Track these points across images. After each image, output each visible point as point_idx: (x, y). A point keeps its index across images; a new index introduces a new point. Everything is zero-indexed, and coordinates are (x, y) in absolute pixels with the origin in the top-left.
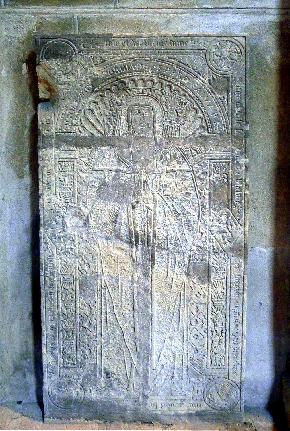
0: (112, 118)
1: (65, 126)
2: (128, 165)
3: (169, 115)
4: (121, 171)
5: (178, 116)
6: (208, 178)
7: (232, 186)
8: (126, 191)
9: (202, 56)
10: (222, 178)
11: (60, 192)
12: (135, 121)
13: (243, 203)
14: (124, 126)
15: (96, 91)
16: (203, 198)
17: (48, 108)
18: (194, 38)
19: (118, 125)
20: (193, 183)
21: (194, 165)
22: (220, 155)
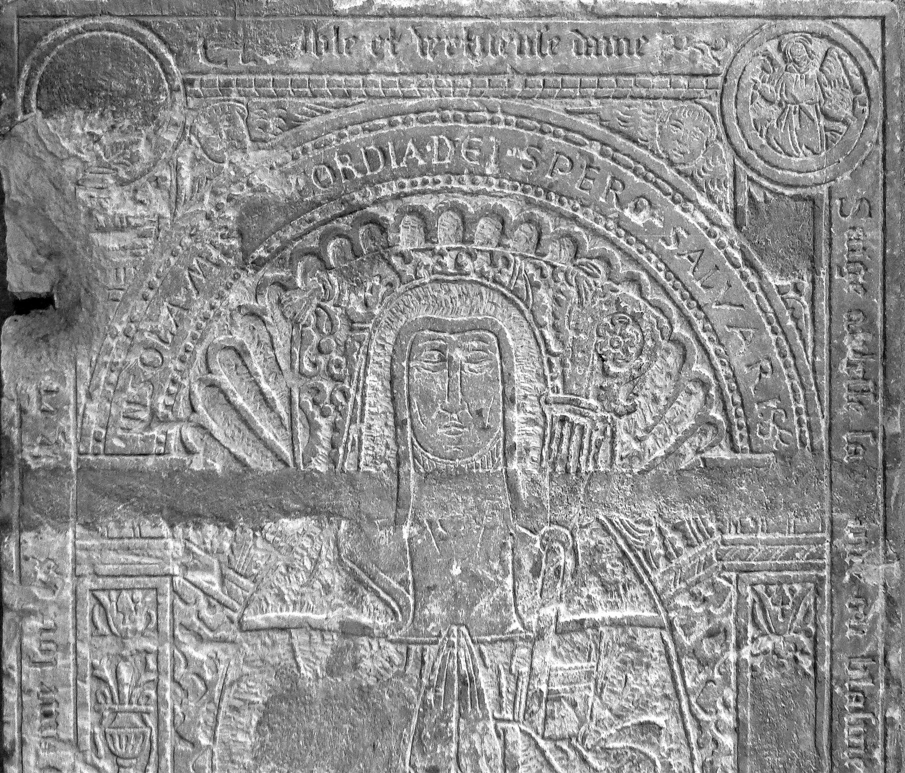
0: (328, 387)
1: (124, 422)
2: (393, 604)
3: (569, 370)
4: (365, 630)
5: (605, 373)
6: (732, 656)
7: (832, 689)
8: (382, 724)
9: (705, 101)
10: (790, 654)
11: (97, 730)
12: (426, 399)
13: (880, 762)
14: (377, 424)
15: (258, 264)
16: (711, 746)
17: (45, 338)
18: (674, 23)
19: (353, 421)
20: (669, 679)
21: (672, 598)
22: (780, 551)
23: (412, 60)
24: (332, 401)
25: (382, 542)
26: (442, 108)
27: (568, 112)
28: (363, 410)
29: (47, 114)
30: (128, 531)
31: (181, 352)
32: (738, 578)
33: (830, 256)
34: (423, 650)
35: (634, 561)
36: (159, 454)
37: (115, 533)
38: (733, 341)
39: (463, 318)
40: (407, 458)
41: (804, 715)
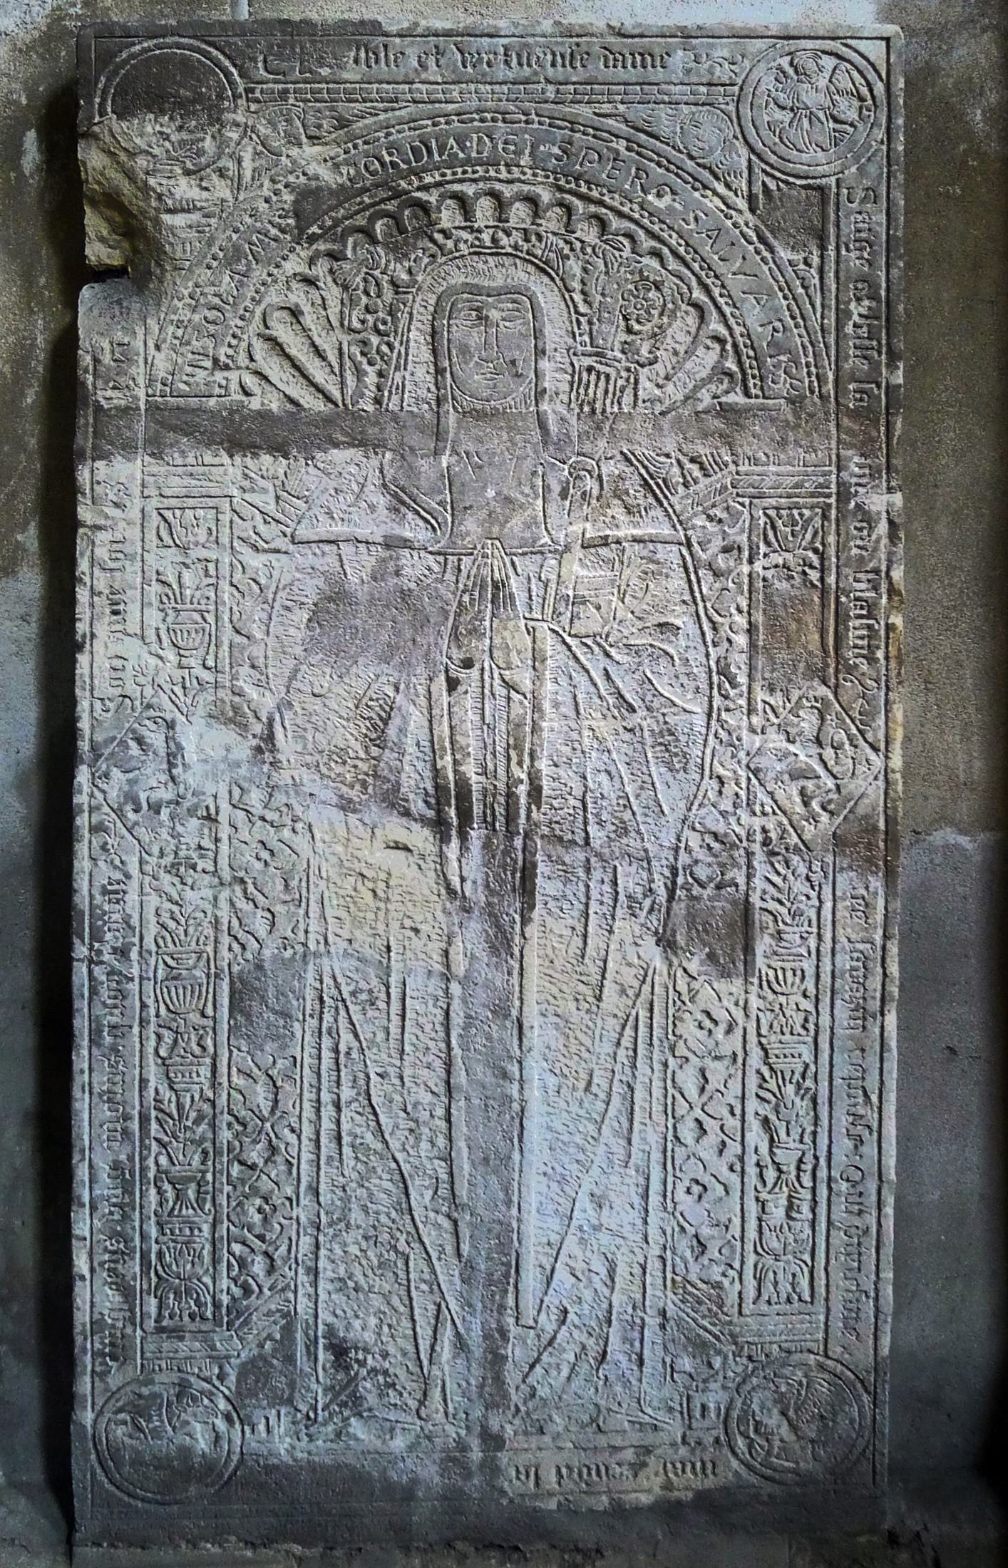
0: (375, 340)
1: (189, 370)
2: (433, 521)
3: (595, 328)
4: (406, 544)
5: (629, 331)
6: (746, 569)
7: (837, 598)
8: (421, 622)
9: (723, 106)
10: (800, 569)
11: (161, 626)
12: (465, 350)
13: (883, 662)
14: (421, 372)
15: (313, 239)
16: (726, 645)
17: (119, 302)
18: (694, 41)
19: (397, 368)
20: (686, 587)
21: (690, 519)
22: (790, 481)
23: (453, 72)
24: (378, 352)
25: (423, 469)
26: (479, 111)
27: (595, 114)
28: (406, 360)
29: (121, 117)
30: (191, 460)
31: (241, 312)
32: (751, 503)
33: (838, 236)
34: (460, 560)
35: (655, 487)
36: (220, 396)
37: (179, 461)
38: (747, 305)
39: (499, 282)
40: (446, 400)
41: (811, 620)
